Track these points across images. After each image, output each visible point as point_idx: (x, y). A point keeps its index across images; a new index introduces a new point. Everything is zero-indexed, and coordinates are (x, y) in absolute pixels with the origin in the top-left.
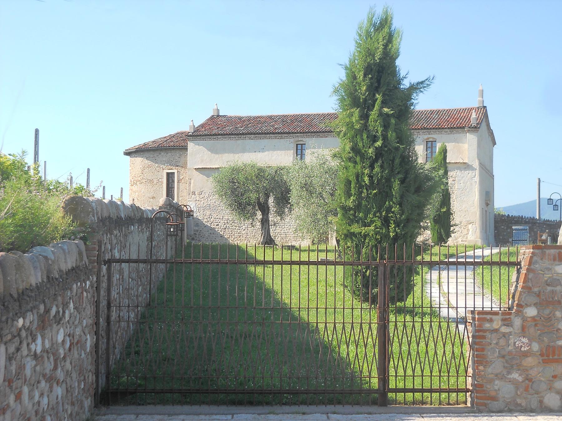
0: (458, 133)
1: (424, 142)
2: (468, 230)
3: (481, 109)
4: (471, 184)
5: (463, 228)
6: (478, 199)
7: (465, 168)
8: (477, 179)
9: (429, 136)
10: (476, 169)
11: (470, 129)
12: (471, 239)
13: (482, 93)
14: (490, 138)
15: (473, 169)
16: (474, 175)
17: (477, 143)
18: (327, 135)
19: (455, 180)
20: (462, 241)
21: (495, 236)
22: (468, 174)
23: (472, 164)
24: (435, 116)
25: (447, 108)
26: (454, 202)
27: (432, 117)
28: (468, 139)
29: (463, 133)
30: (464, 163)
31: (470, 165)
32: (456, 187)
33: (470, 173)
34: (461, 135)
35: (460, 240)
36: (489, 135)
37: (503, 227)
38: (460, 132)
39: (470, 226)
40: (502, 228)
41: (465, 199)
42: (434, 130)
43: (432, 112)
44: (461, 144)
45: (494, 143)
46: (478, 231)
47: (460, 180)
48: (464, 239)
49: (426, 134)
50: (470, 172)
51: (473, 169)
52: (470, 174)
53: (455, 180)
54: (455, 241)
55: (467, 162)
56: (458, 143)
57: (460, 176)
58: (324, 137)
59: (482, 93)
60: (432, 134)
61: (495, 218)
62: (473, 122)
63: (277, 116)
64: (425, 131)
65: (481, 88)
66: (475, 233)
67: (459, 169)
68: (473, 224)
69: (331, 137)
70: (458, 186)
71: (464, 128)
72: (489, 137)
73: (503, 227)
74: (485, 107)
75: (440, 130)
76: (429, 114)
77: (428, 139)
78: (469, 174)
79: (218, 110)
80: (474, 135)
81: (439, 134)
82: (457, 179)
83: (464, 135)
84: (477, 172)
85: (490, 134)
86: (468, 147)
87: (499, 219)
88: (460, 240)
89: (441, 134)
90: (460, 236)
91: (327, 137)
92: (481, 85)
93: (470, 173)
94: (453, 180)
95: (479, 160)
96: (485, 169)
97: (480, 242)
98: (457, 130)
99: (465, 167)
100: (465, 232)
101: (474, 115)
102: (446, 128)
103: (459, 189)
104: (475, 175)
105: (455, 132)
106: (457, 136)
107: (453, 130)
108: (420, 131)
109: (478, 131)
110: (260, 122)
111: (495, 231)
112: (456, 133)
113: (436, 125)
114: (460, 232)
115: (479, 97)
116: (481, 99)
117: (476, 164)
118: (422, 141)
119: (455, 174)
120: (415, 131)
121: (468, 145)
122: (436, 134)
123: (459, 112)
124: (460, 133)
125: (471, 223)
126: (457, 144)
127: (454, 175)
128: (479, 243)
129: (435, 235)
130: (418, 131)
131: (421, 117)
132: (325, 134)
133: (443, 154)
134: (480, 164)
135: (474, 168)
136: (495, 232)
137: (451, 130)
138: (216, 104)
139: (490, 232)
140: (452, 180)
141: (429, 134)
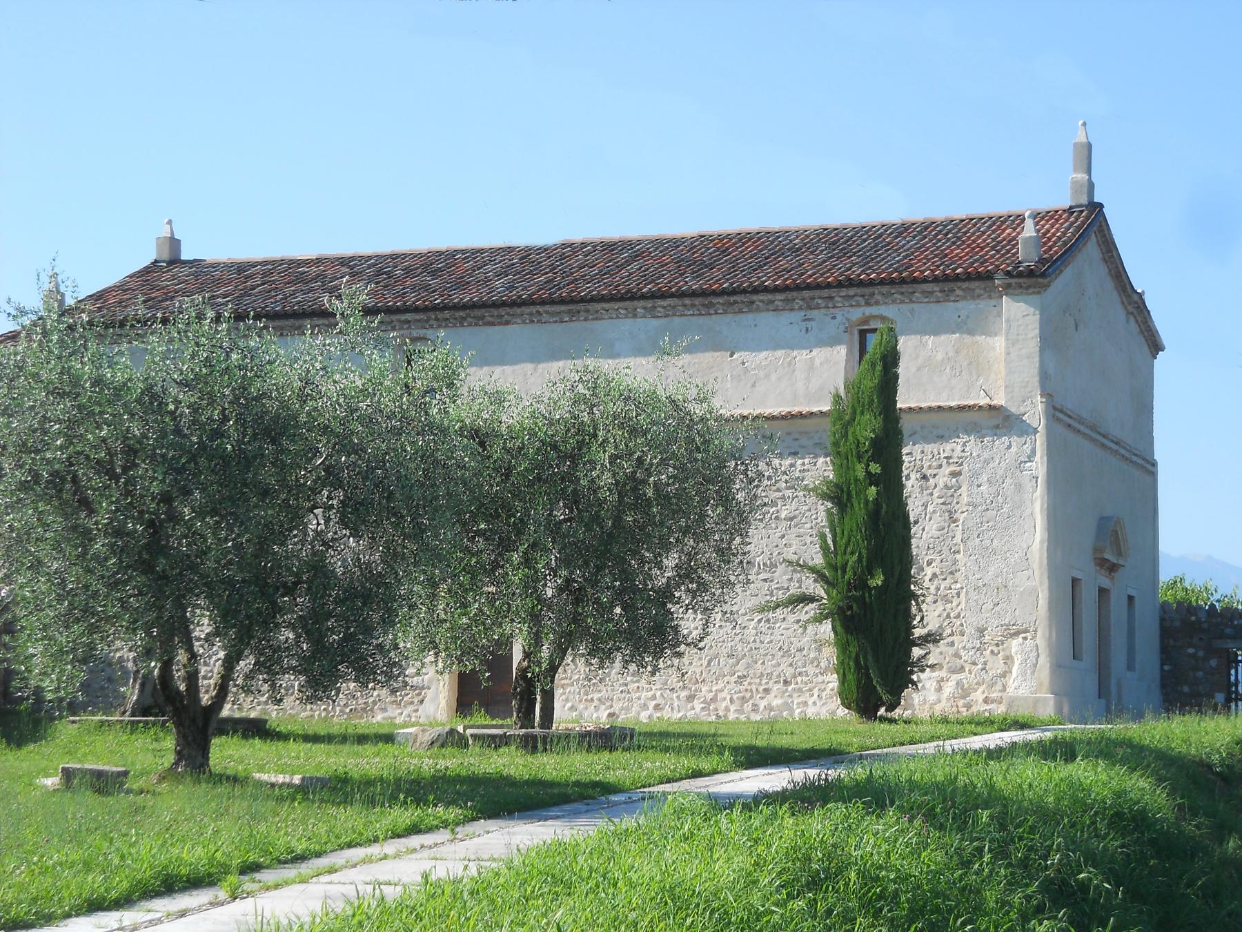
0: (973, 298)
1: (852, 334)
2: (1008, 659)
3: (1082, 211)
4: (1019, 487)
5: (988, 652)
6: (1042, 542)
7: (997, 427)
8: (1039, 466)
9: (869, 311)
10: (1035, 431)
11: (1013, 281)
12: (1021, 692)
13: (1085, 155)
14: (1132, 320)
15: (1030, 431)
16: (1027, 448)
17: (1037, 331)
18: (508, 314)
19: (959, 474)
20: (986, 701)
21: (1163, 686)
22: (1005, 449)
23: (1022, 410)
24: (908, 242)
25: (959, 213)
26: (957, 556)
27: (898, 243)
28: (1008, 321)
29: (990, 297)
30: (991, 408)
31: (1013, 415)
32: (965, 499)
33: (1016, 446)
34: (982, 304)
35: (978, 696)
36: (1129, 313)
37: (1191, 651)
38: (978, 291)
39: (1015, 644)
40: (1190, 655)
41: (995, 541)
42: (885, 289)
43: (904, 229)
44: (981, 339)
45: (1155, 346)
46: (1044, 661)
47: (976, 474)
48: (994, 695)
49: (858, 305)
50: (1015, 440)
51: (1030, 431)
52: (1013, 449)
53: (959, 474)
54: (961, 703)
55: (1003, 403)
56: (971, 332)
57: (978, 456)
58: (500, 324)
59: (1085, 155)
60: (877, 303)
61: (1162, 620)
62: (1026, 254)
63: (369, 258)
64: (852, 291)
65: (1082, 138)
66: (1033, 673)
67: (974, 429)
68: (1025, 638)
69: (524, 322)
70: (969, 496)
71: (989, 276)
72: (1128, 321)
73: (1191, 651)
74: (1096, 208)
75: (905, 288)
76: (891, 233)
77: (866, 321)
78: (1009, 447)
79: (174, 243)
80: (1026, 302)
81: (902, 302)
82: (965, 467)
83: (993, 302)
84: (1040, 440)
85: (1130, 308)
86: (1007, 348)
87: (1177, 624)
88: (978, 696)
89: (911, 301)
90: (978, 684)
91: (507, 323)
92: (1084, 124)
93: (1014, 444)
94: (954, 474)
95: (1047, 395)
96: (1087, 431)
97: (1052, 703)
98: (965, 285)
99: (995, 422)
100: (997, 666)
101: (1029, 230)
102: (925, 280)
103: (975, 506)
104: (1034, 452)
105: (958, 292)
106: (966, 307)
107: (951, 285)
108: (833, 292)
109: (1048, 286)
110: (301, 279)
111: (1162, 665)
112: (964, 298)
113: (896, 270)
114: (980, 666)
115: (1075, 171)
116: (1082, 176)
117: (1035, 412)
118: (842, 328)
119: (959, 448)
120: (817, 293)
121: (1007, 339)
122: (894, 301)
123: (999, 227)
124: (979, 296)
125: (1017, 633)
126: (968, 339)
127: (955, 455)
128: (1047, 710)
129: (850, 677)
130: (826, 293)
131: (858, 245)
132: (502, 311)
133: (879, 368)
134: (1056, 412)
135: (1029, 425)
136: (1162, 670)
137: (947, 286)
138: (170, 222)
139: (1130, 667)
140: (947, 472)
141: (868, 304)
